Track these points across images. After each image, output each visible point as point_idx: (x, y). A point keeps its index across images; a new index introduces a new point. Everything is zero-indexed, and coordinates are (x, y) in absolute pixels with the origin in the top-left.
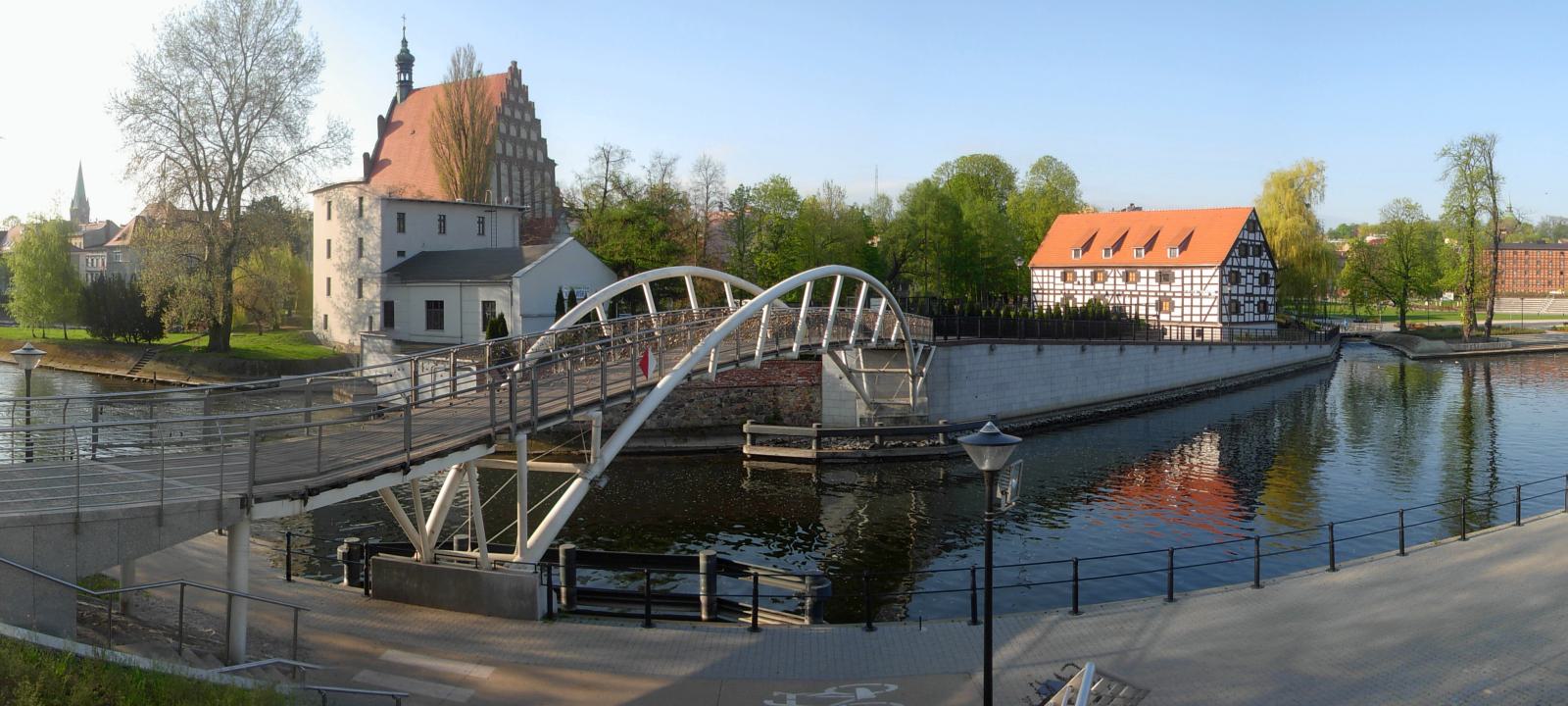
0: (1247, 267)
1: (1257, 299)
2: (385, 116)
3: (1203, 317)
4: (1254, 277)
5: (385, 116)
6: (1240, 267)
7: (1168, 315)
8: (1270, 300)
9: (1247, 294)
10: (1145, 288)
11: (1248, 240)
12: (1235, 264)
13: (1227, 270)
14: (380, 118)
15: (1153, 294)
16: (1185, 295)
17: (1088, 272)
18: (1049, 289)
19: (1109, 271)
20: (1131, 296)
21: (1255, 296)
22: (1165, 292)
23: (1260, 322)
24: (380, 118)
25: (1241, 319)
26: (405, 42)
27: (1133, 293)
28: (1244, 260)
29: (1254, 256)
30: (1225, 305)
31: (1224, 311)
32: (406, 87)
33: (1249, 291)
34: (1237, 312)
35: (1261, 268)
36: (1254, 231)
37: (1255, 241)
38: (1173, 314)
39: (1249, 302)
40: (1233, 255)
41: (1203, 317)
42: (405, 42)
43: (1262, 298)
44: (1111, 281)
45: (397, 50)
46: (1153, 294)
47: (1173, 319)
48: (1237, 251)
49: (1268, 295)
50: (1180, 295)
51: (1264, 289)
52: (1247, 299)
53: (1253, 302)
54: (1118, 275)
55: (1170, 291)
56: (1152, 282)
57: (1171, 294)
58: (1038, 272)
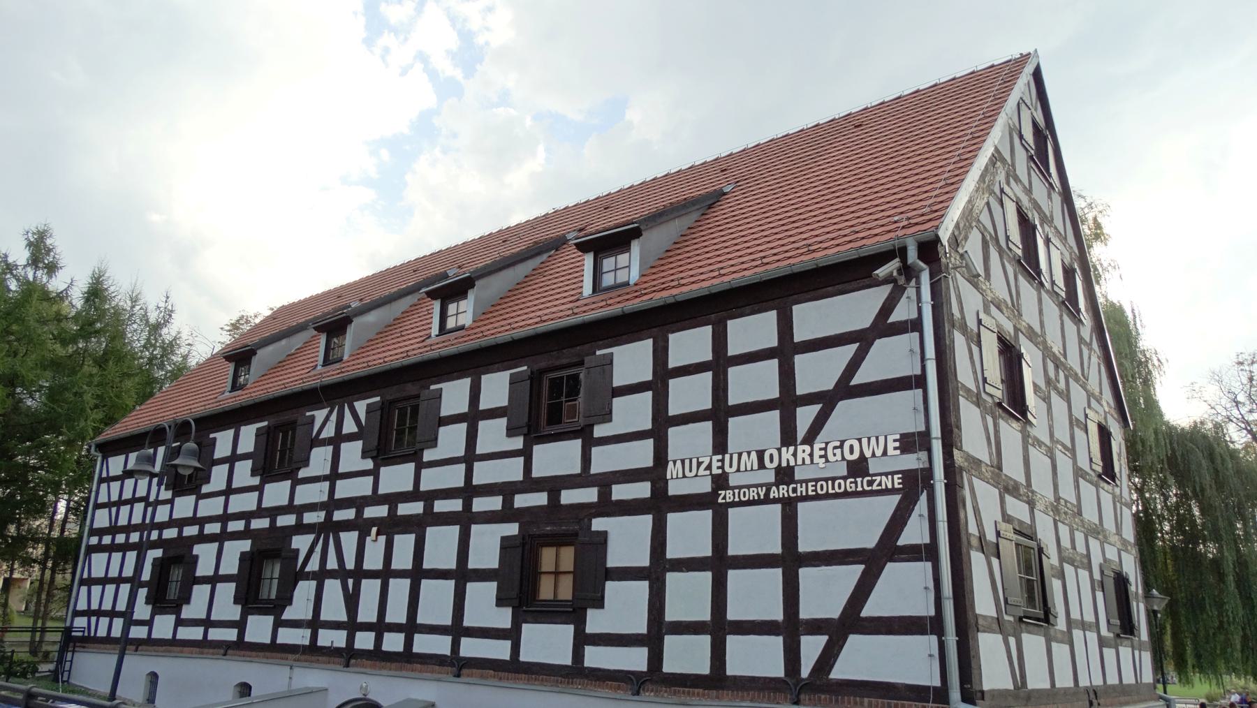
3: (812, 647)
7: (570, 629)
10: (453, 477)
15: (495, 503)
16: (675, 489)
17: (248, 437)
19: (320, 415)
20: (391, 526)
22: (554, 485)
27: (405, 509)
38: (596, 622)
41: (812, 647)
44: (320, 460)
46: (494, 503)
47: (596, 657)
50: (642, 490)
54: (349, 426)
55: (583, 479)
56: (493, 435)
57: (589, 495)
58: (116, 465)
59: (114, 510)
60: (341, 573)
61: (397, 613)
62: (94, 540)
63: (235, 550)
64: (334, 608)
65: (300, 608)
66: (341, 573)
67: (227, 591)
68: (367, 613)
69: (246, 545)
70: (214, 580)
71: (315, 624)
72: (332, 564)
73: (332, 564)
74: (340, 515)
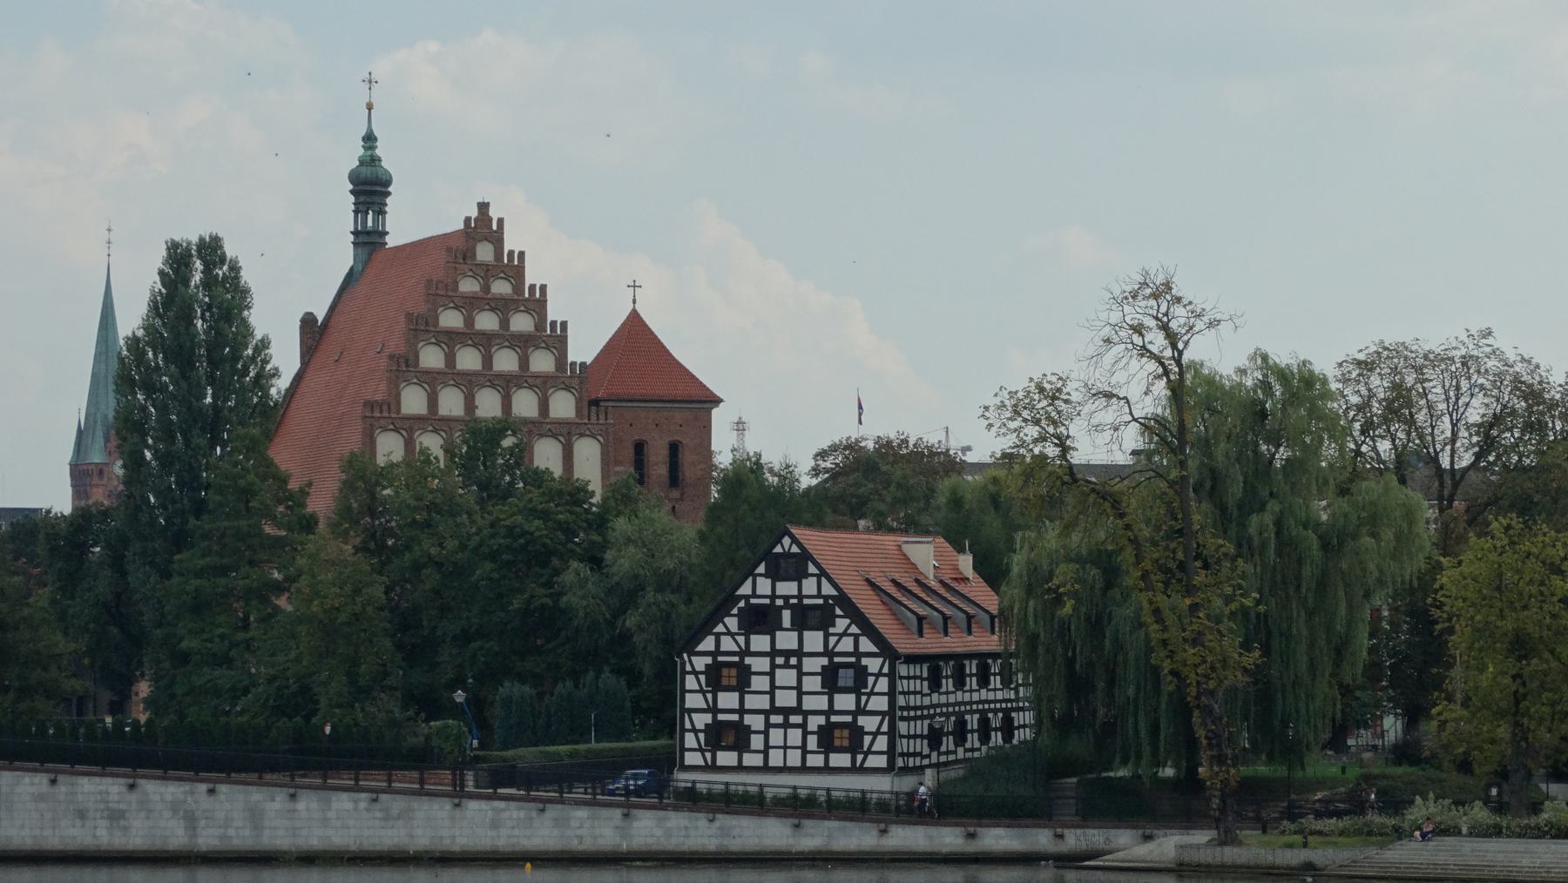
0: (773, 653)
1: (815, 722)
2: (320, 319)
4: (800, 674)
5: (320, 319)
6: (746, 652)
8: (868, 723)
9: (774, 710)
11: (773, 597)
12: (727, 644)
13: (700, 663)
14: (308, 321)
21: (806, 714)
23: (827, 769)
24: (308, 321)
25: (750, 760)
26: (370, 139)
28: (760, 642)
29: (800, 625)
30: (695, 731)
31: (690, 740)
32: (368, 241)
33: (786, 699)
34: (742, 745)
35: (828, 653)
36: (800, 575)
37: (800, 596)
39: (786, 725)
40: (720, 628)
42: (370, 139)
43: (834, 719)
45: (352, 156)
48: (732, 623)
49: (860, 711)
51: (845, 701)
52: (776, 719)
53: (803, 726)
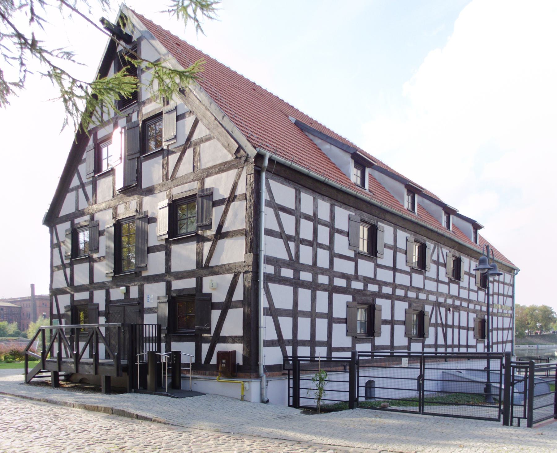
18: (314, 268)
59: (292, 245)
60: (442, 325)
61: (456, 343)
62: (269, 269)
63: (401, 307)
64: (441, 341)
65: (430, 340)
66: (442, 325)
67: (400, 330)
68: (449, 342)
69: (405, 305)
70: (392, 323)
71: (436, 346)
72: (439, 321)
73: (439, 321)
74: (441, 300)
